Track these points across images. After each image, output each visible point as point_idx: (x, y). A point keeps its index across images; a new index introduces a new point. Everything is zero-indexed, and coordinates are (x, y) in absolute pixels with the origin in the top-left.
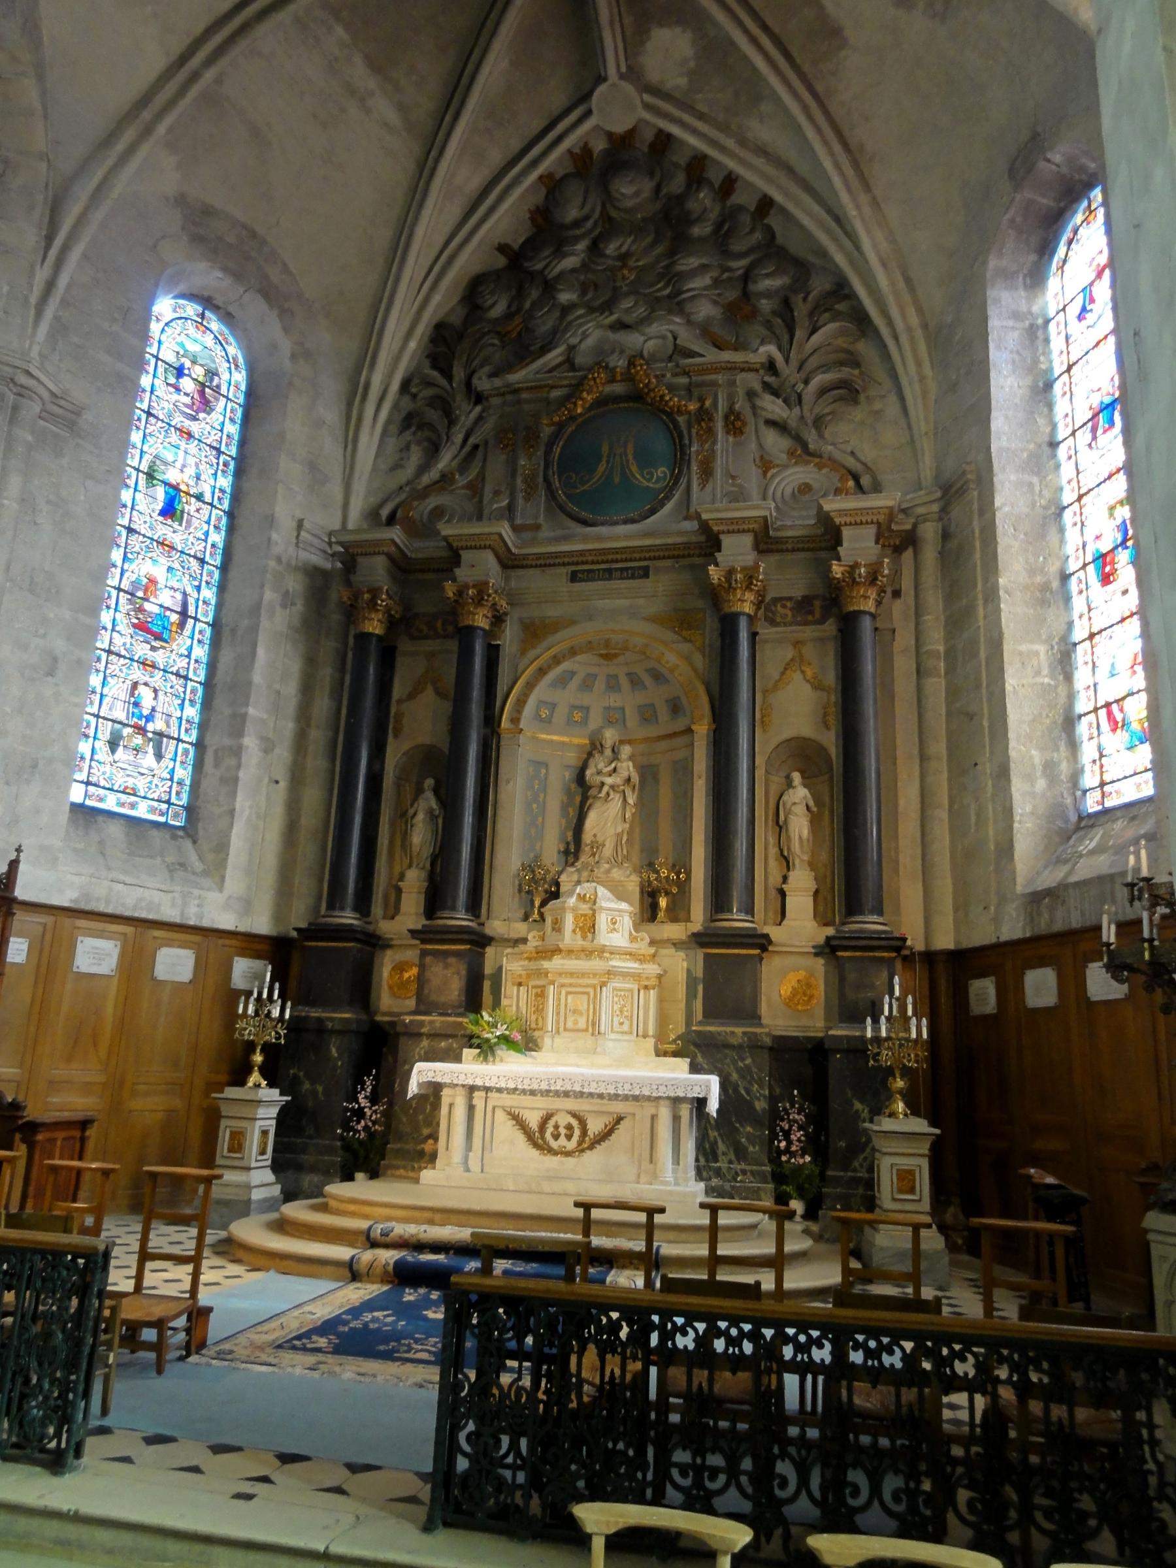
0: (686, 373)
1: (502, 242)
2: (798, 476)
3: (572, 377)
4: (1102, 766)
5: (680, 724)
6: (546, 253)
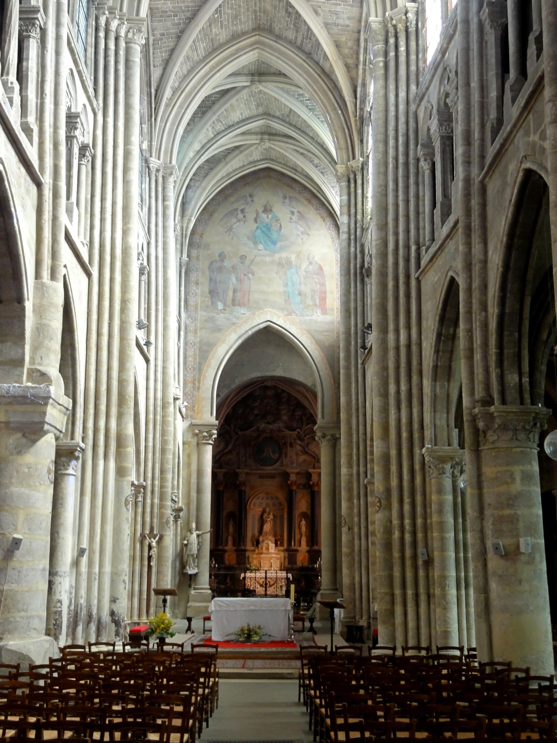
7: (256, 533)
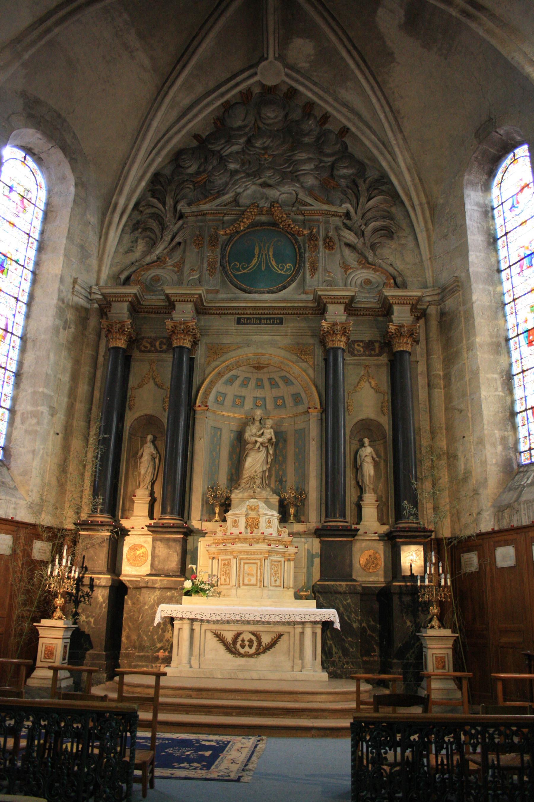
0: (303, 215)
1: (197, 133)
2: (363, 275)
3: (237, 210)
4: (530, 440)
5: (301, 408)
6: (223, 142)
7: (223, 480)
